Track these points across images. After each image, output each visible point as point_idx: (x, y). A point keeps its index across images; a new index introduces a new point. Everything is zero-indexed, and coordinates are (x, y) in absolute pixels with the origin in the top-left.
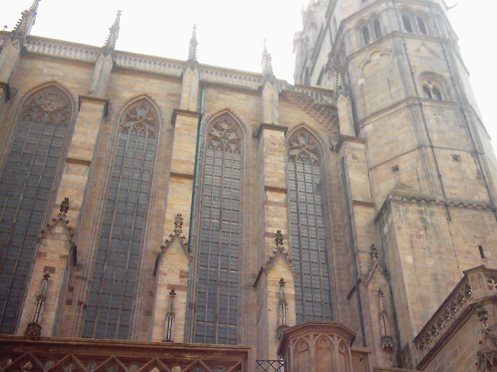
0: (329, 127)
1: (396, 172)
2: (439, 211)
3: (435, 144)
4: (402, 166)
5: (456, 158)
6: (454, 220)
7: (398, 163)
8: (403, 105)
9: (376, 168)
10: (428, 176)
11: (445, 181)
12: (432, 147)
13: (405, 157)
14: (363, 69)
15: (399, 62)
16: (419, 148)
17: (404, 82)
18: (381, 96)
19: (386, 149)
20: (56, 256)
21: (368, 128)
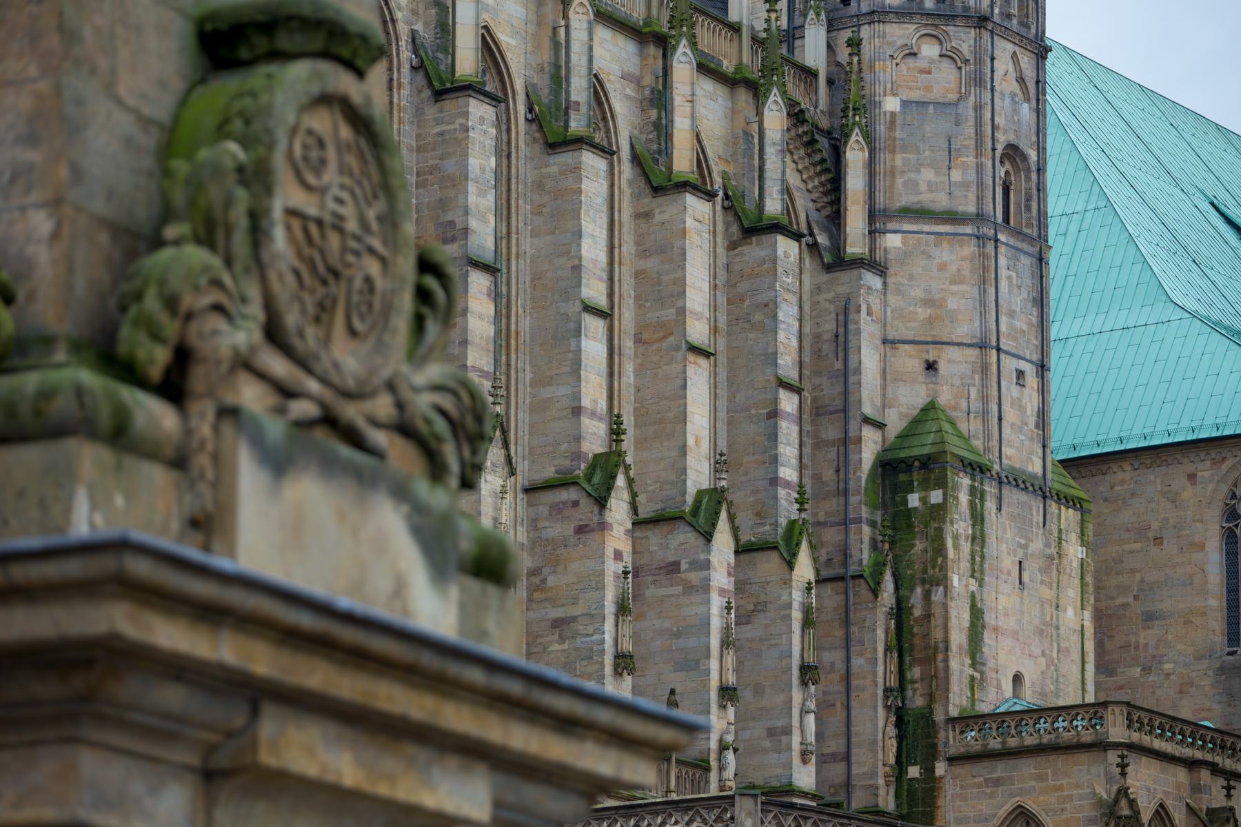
0: (810, 186)
1: (932, 372)
2: (990, 488)
3: (1002, 346)
4: (943, 367)
5: (1020, 374)
6: (1004, 508)
7: (939, 357)
8: (968, 229)
9: (897, 345)
10: (985, 413)
11: (1007, 431)
12: (998, 350)
13: (954, 353)
14: (897, 64)
15: (978, 108)
16: (981, 348)
17: (980, 168)
18: (928, 175)
19: (923, 313)
20: (622, 529)
21: (893, 241)
